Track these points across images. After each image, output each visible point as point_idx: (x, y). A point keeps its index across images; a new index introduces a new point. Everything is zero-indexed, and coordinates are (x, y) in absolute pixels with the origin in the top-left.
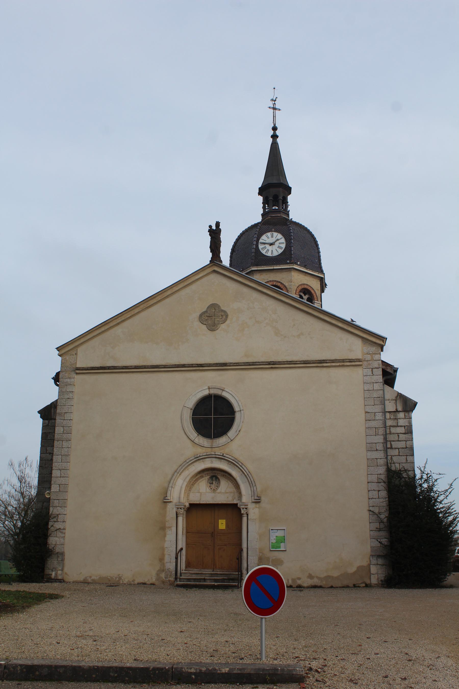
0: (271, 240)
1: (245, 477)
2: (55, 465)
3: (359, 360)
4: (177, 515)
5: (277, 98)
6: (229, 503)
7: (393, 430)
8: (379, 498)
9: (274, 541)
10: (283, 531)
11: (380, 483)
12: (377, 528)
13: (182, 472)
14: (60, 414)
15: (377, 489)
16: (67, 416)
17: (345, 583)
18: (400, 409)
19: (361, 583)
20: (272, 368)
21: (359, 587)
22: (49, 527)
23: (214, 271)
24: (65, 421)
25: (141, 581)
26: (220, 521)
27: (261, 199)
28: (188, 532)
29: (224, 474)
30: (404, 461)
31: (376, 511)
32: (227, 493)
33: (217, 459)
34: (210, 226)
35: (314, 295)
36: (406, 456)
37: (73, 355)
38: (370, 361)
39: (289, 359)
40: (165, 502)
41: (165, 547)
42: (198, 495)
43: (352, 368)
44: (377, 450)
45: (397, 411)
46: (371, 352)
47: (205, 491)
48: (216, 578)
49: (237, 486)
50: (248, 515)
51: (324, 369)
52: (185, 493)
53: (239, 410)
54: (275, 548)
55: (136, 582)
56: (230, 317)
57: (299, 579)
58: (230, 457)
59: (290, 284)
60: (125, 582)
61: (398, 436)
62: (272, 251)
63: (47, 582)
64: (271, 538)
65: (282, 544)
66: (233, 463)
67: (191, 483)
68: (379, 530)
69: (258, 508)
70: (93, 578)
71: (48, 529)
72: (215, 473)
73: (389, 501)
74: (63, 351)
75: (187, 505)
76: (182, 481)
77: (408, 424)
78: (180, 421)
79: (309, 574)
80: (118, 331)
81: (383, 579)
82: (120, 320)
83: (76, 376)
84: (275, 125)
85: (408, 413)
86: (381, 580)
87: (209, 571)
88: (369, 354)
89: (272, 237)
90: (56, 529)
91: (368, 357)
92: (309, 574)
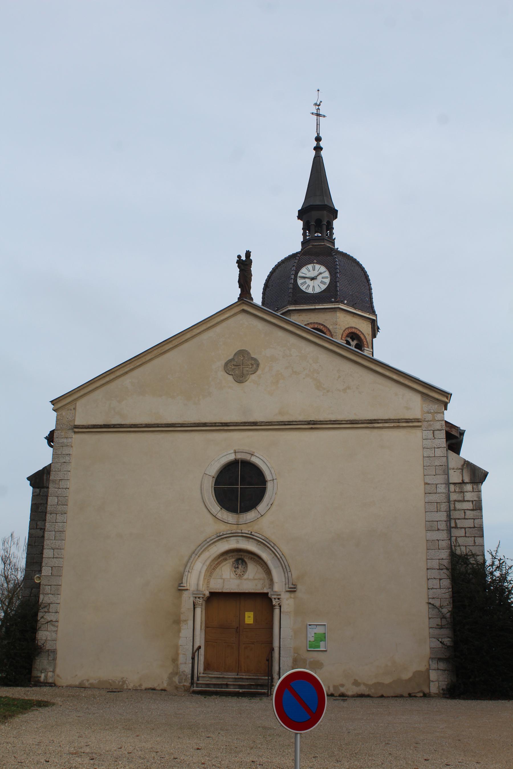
0: (312, 274)
1: (277, 561)
2: (46, 542)
3: (418, 420)
4: (194, 605)
5: (321, 102)
7: (458, 506)
8: (440, 588)
9: (312, 639)
10: (323, 627)
11: (442, 569)
12: (437, 625)
13: (201, 554)
14: (54, 481)
15: (439, 577)
16: (62, 484)
17: (399, 692)
18: (467, 480)
19: (418, 692)
20: (312, 428)
21: (415, 696)
22: (39, 619)
23: (244, 311)
24: (60, 490)
25: (150, 686)
26: (247, 614)
27: (301, 223)
28: (208, 627)
29: (253, 556)
30: (472, 543)
31: (437, 603)
32: (256, 579)
33: (244, 539)
34: (239, 257)
35: (364, 340)
36: (474, 537)
37: (71, 410)
38: (431, 421)
39: (333, 418)
40: (180, 590)
41: (179, 644)
42: (220, 581)
43: (409, 430)
44: (438, 530)
45: (463, 483)
46: (432, 411)
47: (229, 577)
48: (241, 683)
49: (268, 572)
50: (280, 606)
51: (376, 432)
52: (204, 579)
53: (272, 479)
54: (313, 647)
55: (143, 687)
56: (261, 366)
57: (342, 685)
58: (260, 536)
59: (335, 327)
60: (130, 687)
61: (465, 512)
62: (314, 287)
63: (35, 685)
64: (309, 635)
65: (322, 644)
66: (264, 543)
67: (212, 567)
68: (441, 627)
69: (294, 598)
70: (91, 681)
71: (37, 621)
72: (241, 555)
73: (453, 593)
74: (59, 405)
75: (207, 594)
76: (202, 565)
77: (477, 499)
78: (199, 491)
79: (355, 680)
80: (127, 381)
81: (444, 687)
82: (129, 369)
83: (75, 436)
84: (318, 134)
85: (477, 485)
86: (443, 689)
87: (232, 675)
88: (430, 413)
89: (314, 270)
90: (46, 621)
91: (429, 417)
92: (355, 680)
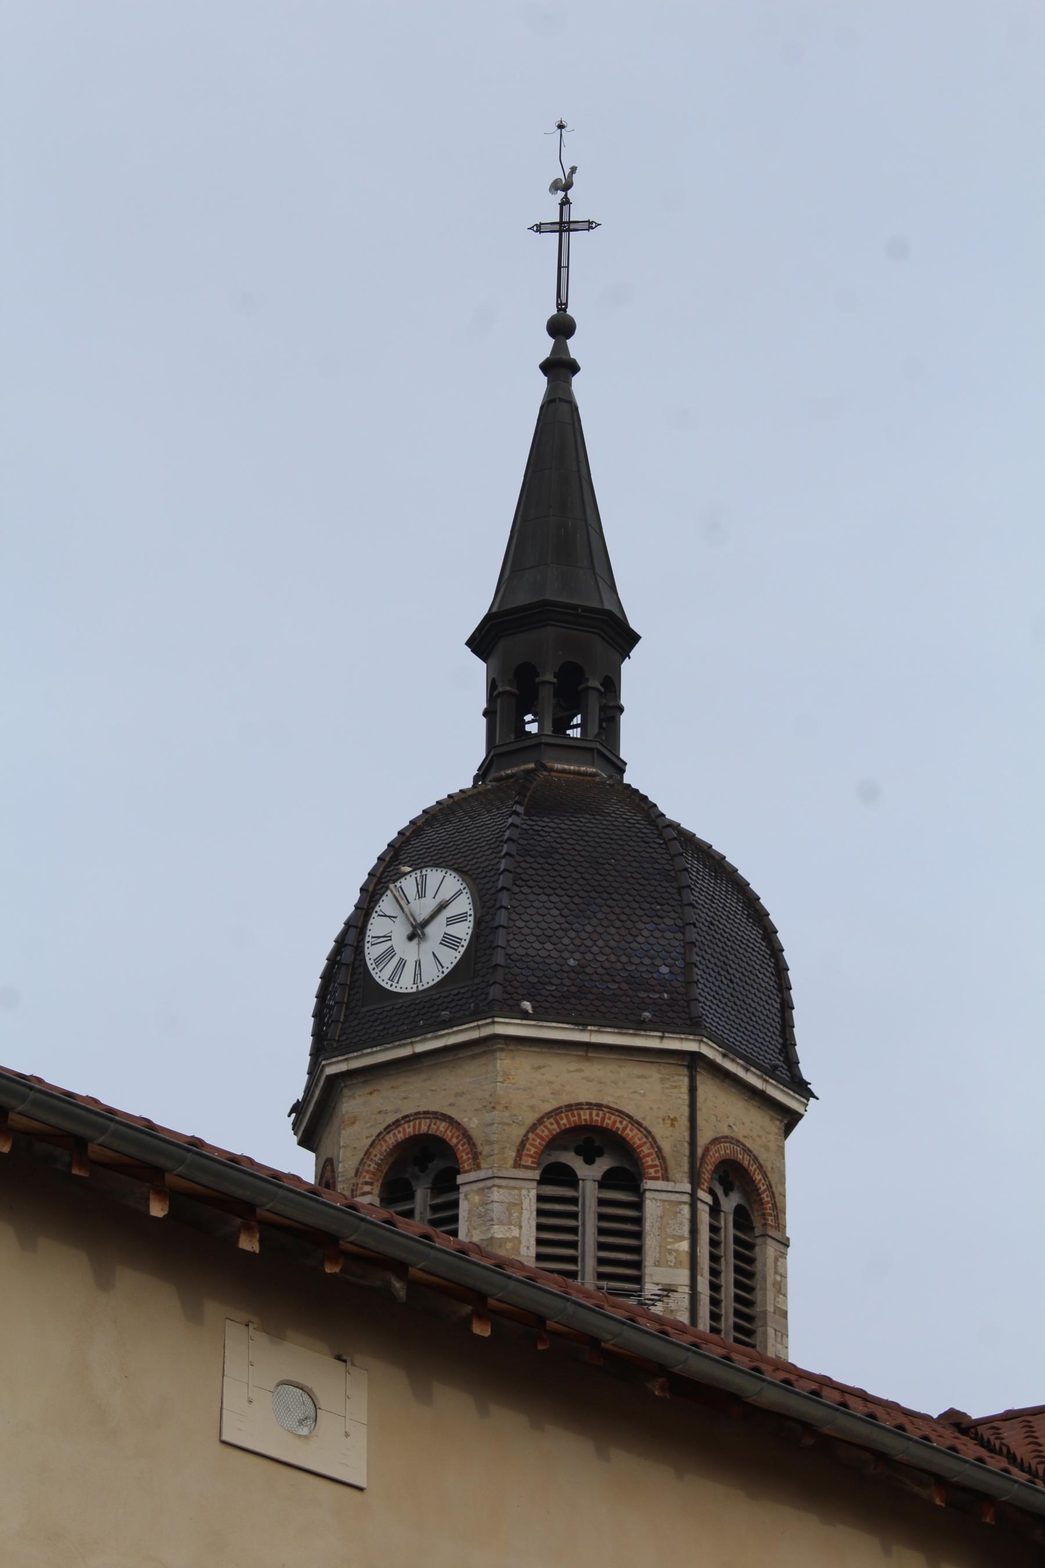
59: (488, 1117)
62: (418, 964)
84: (562, 306)
89: (421, 894)
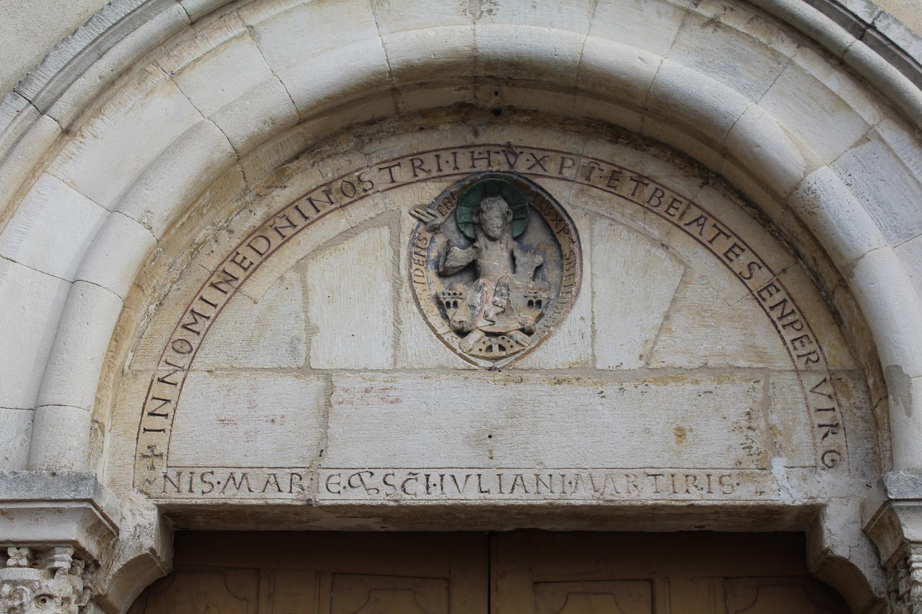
6: (697, 497)
13: (90, 107)
29: (625, 157)
32: (676, 375)
42: (294, 396)
47: (381, 358)
67: (212, 263)
72: (509, 150)
75: (138, 526)
76: (96, 214)
